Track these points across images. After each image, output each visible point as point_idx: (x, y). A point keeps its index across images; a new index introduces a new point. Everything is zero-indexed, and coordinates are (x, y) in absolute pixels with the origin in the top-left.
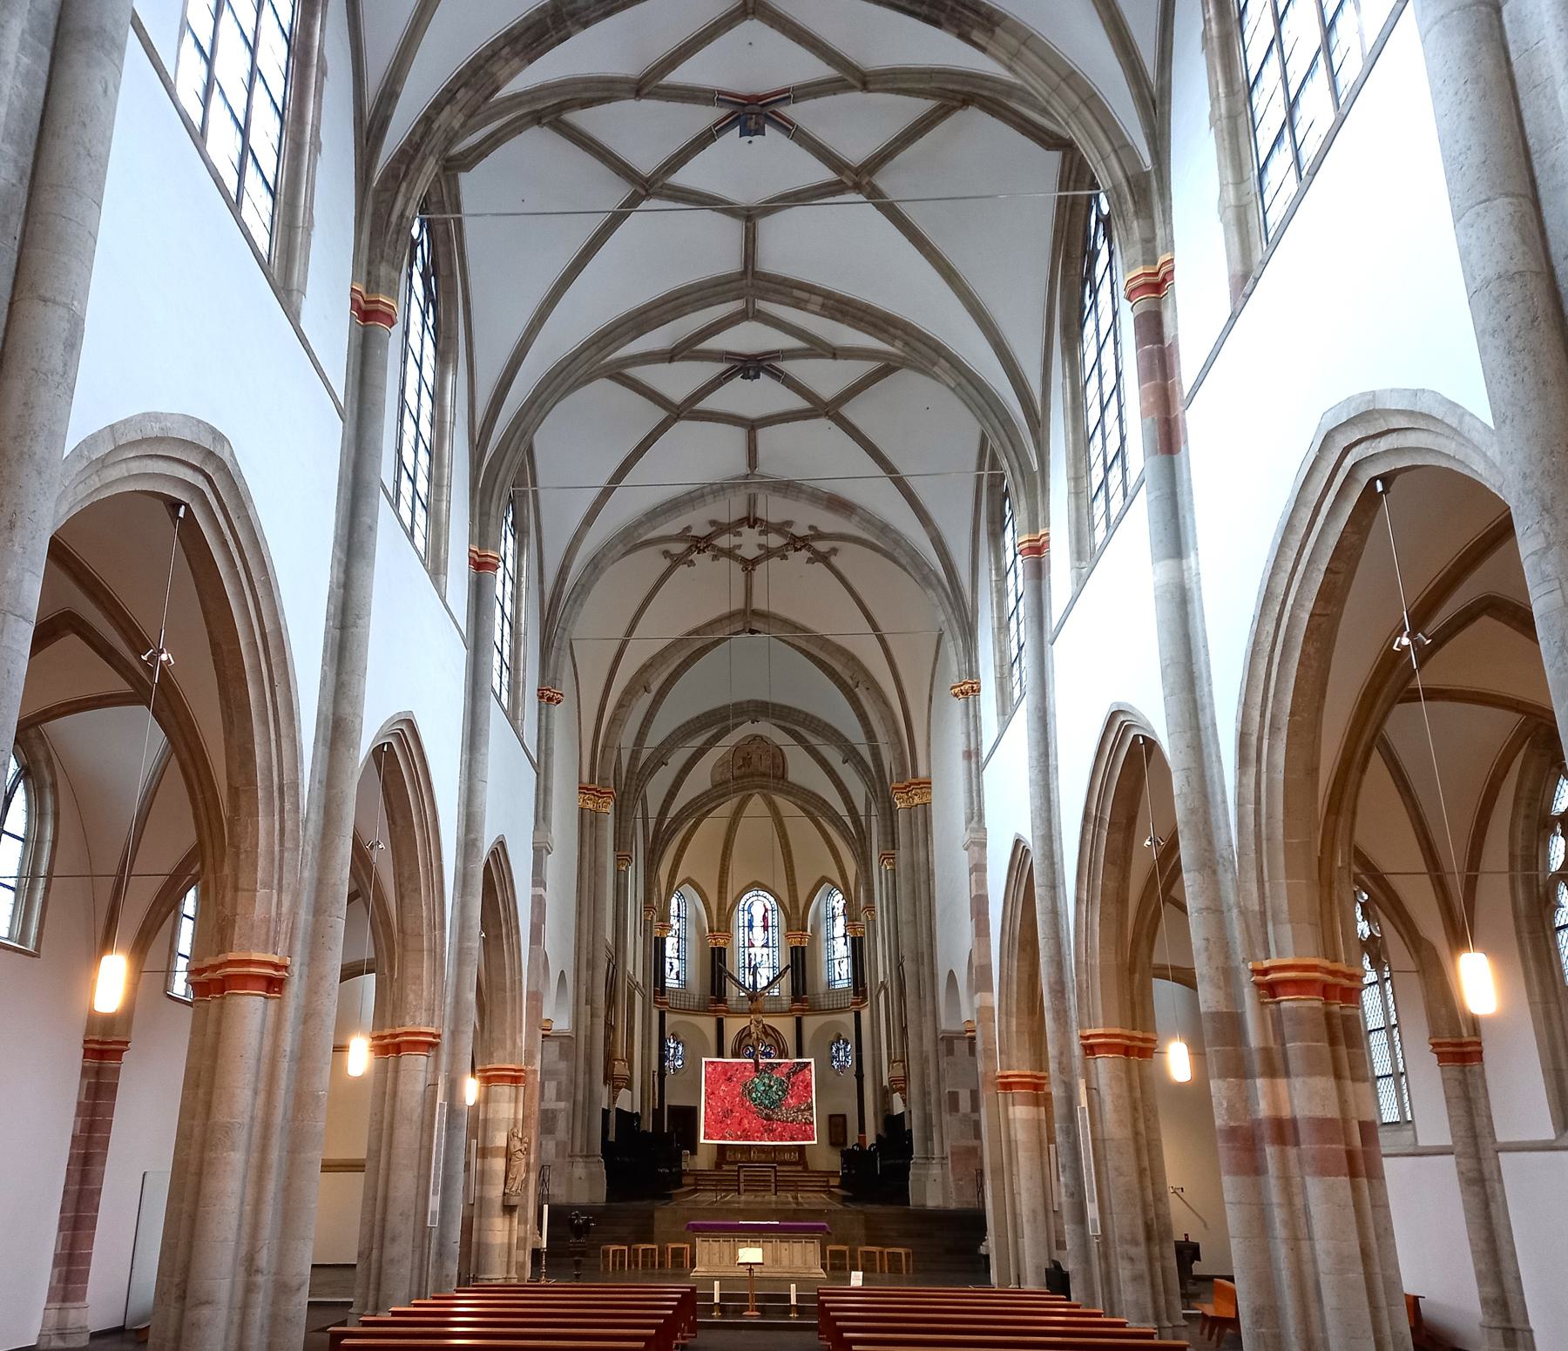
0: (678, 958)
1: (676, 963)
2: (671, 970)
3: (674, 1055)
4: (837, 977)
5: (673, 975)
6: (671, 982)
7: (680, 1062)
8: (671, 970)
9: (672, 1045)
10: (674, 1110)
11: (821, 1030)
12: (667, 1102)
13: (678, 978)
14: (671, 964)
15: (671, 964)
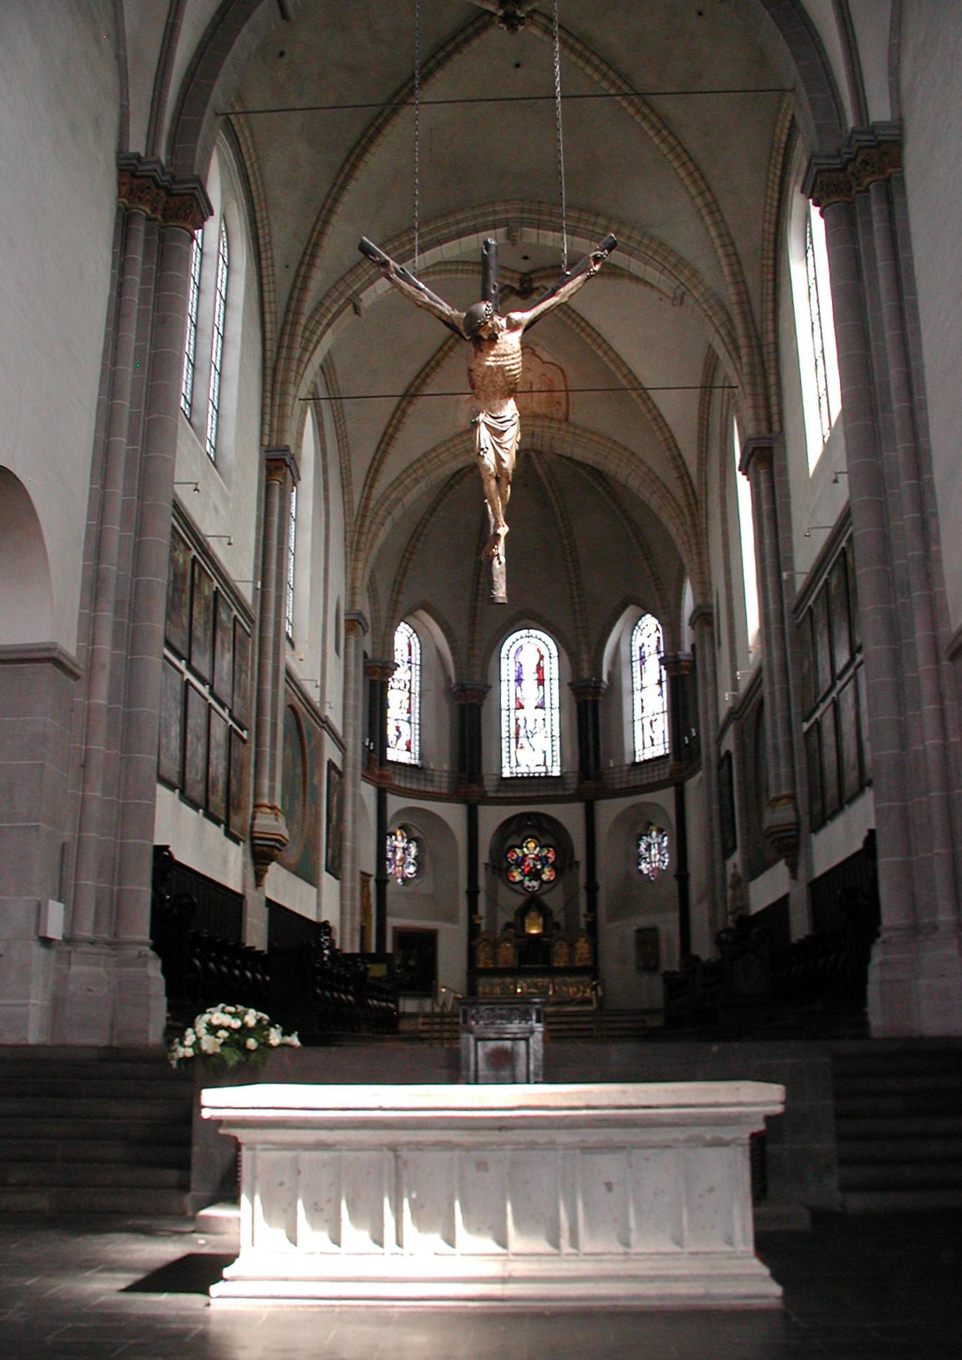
0: (409, 722)
1: (405, 728)
2: (398, 737)
3: (403, 860)
4: (648, 743)
5: (402, 744)
6: (396, 753)
7: (412, 869)
8: (398, 737)
9: (400, 843)
10: (404, 937)
11: (623, 818)
12: (392, 922)
13: (409, 749)
14: (398, 729)
15: (398, 729)
